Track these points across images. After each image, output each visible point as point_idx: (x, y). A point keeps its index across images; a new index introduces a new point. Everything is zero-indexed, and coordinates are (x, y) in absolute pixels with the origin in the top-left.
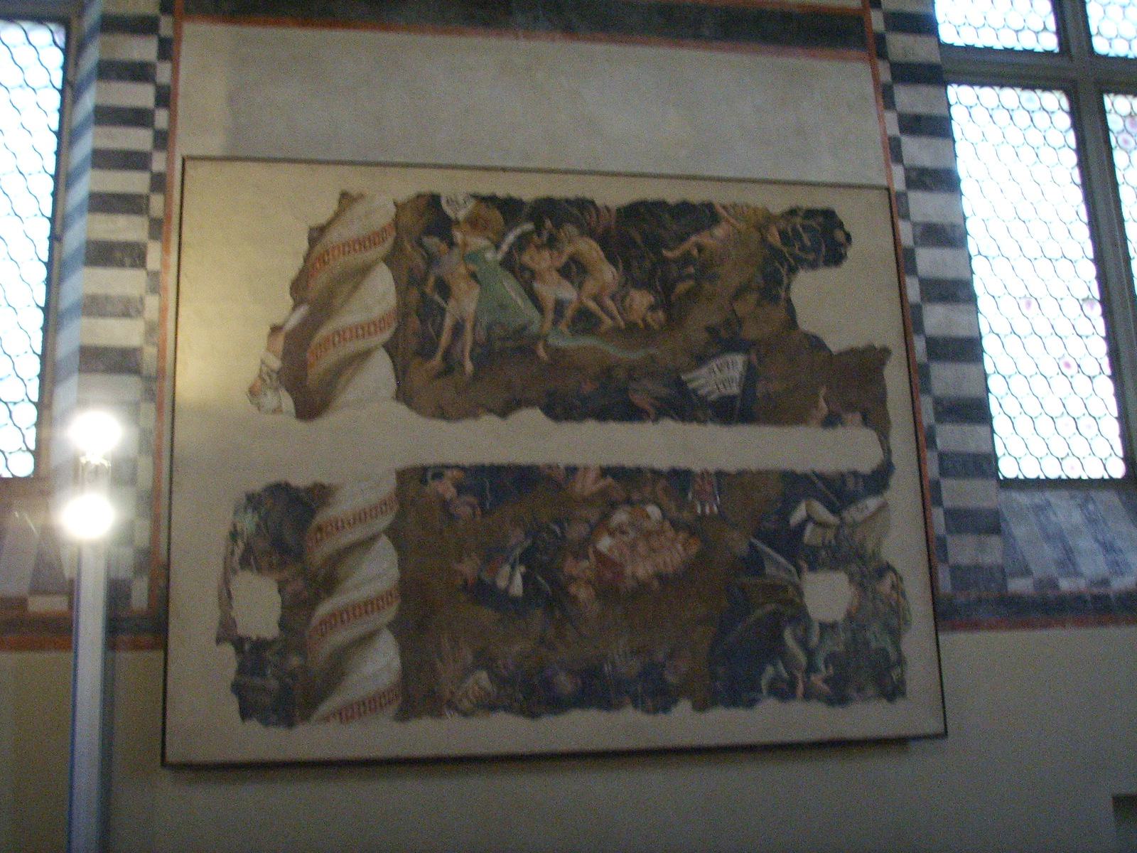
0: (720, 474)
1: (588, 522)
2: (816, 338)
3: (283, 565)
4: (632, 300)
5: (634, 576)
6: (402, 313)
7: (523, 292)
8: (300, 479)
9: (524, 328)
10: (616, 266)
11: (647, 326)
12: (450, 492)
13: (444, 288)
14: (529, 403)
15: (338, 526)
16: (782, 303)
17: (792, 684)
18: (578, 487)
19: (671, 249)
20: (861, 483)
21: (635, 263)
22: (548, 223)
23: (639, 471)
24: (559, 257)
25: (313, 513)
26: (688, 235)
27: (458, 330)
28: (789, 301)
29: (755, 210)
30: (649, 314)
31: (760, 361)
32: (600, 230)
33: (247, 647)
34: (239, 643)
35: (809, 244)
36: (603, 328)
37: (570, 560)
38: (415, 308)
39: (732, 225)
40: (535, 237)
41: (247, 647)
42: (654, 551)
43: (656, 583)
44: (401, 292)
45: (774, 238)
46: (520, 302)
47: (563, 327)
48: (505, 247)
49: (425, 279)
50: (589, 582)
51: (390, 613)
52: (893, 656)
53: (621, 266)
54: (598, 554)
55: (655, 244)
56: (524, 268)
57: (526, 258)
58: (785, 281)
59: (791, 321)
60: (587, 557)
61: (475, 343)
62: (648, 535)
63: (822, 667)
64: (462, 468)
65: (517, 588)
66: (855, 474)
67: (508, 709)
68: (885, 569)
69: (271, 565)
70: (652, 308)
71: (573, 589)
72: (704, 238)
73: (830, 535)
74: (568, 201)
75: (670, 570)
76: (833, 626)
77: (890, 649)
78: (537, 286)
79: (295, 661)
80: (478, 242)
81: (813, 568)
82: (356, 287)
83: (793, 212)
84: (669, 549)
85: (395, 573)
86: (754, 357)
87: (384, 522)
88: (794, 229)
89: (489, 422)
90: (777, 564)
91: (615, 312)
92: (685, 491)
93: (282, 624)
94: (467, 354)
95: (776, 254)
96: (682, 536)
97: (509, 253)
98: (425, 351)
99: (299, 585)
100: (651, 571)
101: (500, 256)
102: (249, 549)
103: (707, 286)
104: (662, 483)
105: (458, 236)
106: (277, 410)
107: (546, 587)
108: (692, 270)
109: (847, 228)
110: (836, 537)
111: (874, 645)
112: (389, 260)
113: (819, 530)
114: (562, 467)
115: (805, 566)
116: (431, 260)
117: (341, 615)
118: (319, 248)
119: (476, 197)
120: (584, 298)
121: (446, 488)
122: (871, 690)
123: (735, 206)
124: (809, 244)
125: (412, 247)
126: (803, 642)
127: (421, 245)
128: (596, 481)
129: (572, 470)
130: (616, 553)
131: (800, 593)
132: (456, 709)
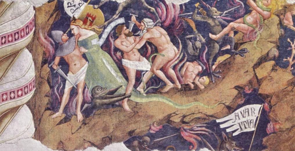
4: (187, 68)
6: (39, 81)
10: (178, 48)
11: (196, 87)
13: (65, 65)
22: (134, 18)
26: (229, 22)
27: (74, 92)
36: (166, 89)
38: (46, 78)
40: (125, 28)
44: (38, 69)
46: (113, 73)
47: (140, 89)
48: (105, 36)
53: (181, 46)
56: (116, 50)
70: (201, 74)
80: (87, 33)
98: (53, 107)
101: (102, 42)
105: (75, 30)
112: (30, 47)
116: (58, 46)
125: (46, 38)
127: (50, 35)
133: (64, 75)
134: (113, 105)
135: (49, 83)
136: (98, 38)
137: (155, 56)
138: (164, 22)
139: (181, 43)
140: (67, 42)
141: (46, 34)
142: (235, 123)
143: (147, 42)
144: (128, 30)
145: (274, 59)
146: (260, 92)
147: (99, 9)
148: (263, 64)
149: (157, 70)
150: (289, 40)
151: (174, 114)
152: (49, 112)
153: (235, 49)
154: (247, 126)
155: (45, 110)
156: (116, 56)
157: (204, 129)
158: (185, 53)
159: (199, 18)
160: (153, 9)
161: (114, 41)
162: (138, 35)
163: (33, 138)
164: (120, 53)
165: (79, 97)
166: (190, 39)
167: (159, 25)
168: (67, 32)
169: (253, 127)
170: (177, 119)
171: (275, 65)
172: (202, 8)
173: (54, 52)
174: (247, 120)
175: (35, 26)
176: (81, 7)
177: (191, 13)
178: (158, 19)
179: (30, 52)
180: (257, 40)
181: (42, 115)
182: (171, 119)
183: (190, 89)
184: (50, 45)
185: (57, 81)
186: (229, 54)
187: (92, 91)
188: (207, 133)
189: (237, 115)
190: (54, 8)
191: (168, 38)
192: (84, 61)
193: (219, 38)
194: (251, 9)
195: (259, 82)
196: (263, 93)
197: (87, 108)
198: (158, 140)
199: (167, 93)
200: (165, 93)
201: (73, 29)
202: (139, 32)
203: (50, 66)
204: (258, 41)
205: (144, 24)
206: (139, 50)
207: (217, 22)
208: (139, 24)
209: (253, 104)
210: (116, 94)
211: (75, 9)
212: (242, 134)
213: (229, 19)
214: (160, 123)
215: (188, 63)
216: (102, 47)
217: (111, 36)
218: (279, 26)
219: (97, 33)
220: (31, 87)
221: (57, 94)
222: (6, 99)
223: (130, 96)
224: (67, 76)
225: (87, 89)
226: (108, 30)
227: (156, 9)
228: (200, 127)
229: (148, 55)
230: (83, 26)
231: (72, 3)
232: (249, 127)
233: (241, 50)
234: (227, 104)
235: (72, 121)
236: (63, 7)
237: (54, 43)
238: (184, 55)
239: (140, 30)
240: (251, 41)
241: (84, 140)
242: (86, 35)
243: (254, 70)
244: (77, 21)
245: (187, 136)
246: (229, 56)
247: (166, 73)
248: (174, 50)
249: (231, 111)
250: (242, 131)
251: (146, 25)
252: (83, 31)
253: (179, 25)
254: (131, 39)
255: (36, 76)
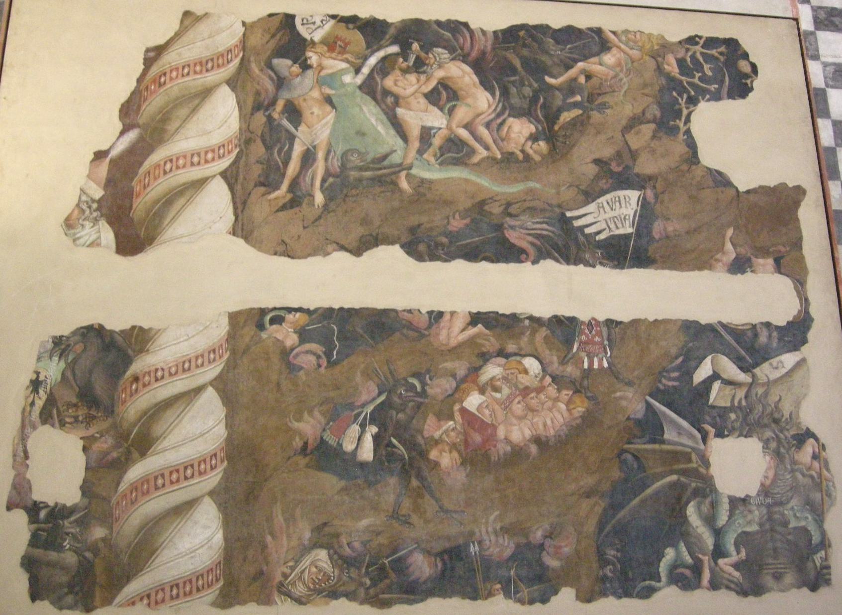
0: (609, 323)
1: (454, 376)
2: (720, 173)
3: (90, 420)
4: (510, 127)
5: (507, 440)
6: (245, 139)
7: (384, 117)
8: (116, 323)
9: (385, 157)
10: (493, 94)
11: (527, 157)
12: (292, 339)
13: (294, 113)
14: (390, 242)
15: (158, 375)
16: (681, 137)
17: (697, 569)
18: (443, 336)
19: (555, 77)
20: (775, 334)
21: (513, 90)
22: (415, 46)
23: (514, 317)
24: (428, 79)
25: (127, 361)
26: (576, 61)
27: (308, 158)
28: (688, 132)
29: (650, 35)
30: (529, 143)
31: (656, 196)
32: (474, 54)
33: (43, 514)
34: (33, 509)
35: (710, 73)
36: (476, 159)
37: (431, 420)
38: (259, 134)
39: (625, 53)
40: (401, 60)
41: (43, 514)
42: (532, 410)
43: (534, 449)
44: (245, 117)
45: (672, 66)
46: (380, 128)
47: (428, 156)
48: (366, 70)
49: (273, 103)
50: (454, 446)
51: (213, 479)
52: (816, 539)
53: (498, 93)
54: (464, 411)
55: (537, 69)
56: (386, 93)
57: (389, 82)
58: (685, 112)
59: (693, 156)
60: (451, 417)
61: (328, 174)
62: (526, 391)
63: (732, 549)
64: (308, 312)
65: (367, 452)
66: (768, 325)
67: (350, 596)
68: (805, 436)
69: (76, 418)
70: (534, 138)
71: (433, 455)
72: (591, 65)
73: (741, 393)
74: (438, 23)
75: (552, 432)
76: (745, 501)
77: (812, 528)
78: (400, 111)
79: (98, 533)
80: (334, 64)
81: (720, 435)
82: (194, 110)
83: (692, 40)
84: (550, 410)
85: (221, 431)
86: (649, 193)
87: (213, 371)
88: (693, 57)
89: (341, 258)
90: (680, 430)
91: (490, 141)
92: (569, 343)
93: (86, 489)
94: (318, 183)
95: (673, 84)
96: (566, 394)
97: (371, 76)
98: (269, 183)
99: (105, 444)
100: (528, 433)
101: (359, 79)
102: (51, 401)
103: (596, 116)
104: (543, 332)
105: (313, 58)
106: (95, 244)
107: (402, 449)
108: (578, 98)
109: (752, 59)
110: (746, 397)
111: (793, 524)
112: (232, 83)
113: (728, 390)
114: (424, 311)
115: (712, 431)
116: (281, 82)
117: (156, 478)
118: (155, 70)
119: (333, 17)
120: (454, 126)
121: (286, 334)
122: (789, 579)
123: (626, 32)
124: (710, 73)
125: (261, 70)
126: (710, 520)
127: (270, 66)
128: (463, 330)
129: (436, 316)
130: (487, 412)
131: (707, 465)
132: (289, 595)
133: (293, 130)
134: (380, 181)
135: (264, 141)
136: (354, 72)
137: (455, 106)
138: (469, 54)
139: (499, 87)
140: (299, 78)
141: (262, 64)
142: (599, 219)
143: (439, 83)
144: (406, 63)
145: (654, 121)
146: (637, 170)
147: (356, 30)
148: (637, 128)
149: (458, 127)
150: (675, 94)
151: (491, 201)
152: (262, 189)
153: (588, 101)
154: (620, 225)
155: (256, 186)
156: (384, 102)
157: (545, 226)
158: (506, 104)
159: (525, 52)
160: (449, 35)
161: (382, 79)
162: (424, 72)
163: (230, 233)
164: (392, 98)
165: (317, 167)
166: (513, 82)
167: (459, 60)
168: (299, 62)
169: (630, 227)
170: (496, 209)
171: (655, 132)
172: (529, 37)
173: (275, 90)
174: (619, 216)
175: (244, 51)
176: (326, 26)
177: (513, 44)
178: (457, 50)
179: (233, 90)
180: (623, 91)
181: (250, 194)
182: (486, 208)
183: (517, 161)
184: (267, 79)
185: (279, 140)
186: (579, 108)
187: (342, 158)
188: (550, 234)
189: (601, 205)
190: (277, 24)
191: (476, 79)
192: (328, 108)
193: (561, 84)
194: (609, 45)
195: (634, 155)
196: (640, 172)
197: (331, 185)
198: (464, 242)
199: (478, 164)
200: (474, 164)
201: (310, 58)
202: (425, 68)
203: (267, 114)
204: (625, 92)
205: (435, 57)
206: (426, 96)
207: (556, 60)
208: (426, 56)
209: (626, 189)
210: (386, 163)
211: (313, 27)
212: (613, 237)
213: (576, 56)
214: (466, 213)
215: (511, 119)
216: (360, 87)
217: (377, 73)
218: (657, 73)
219: (351, 65)
220: (230, 147)
221: (279, 160)
222: (184, 166)
223: (410, 167)
224: (297, 130)
225: (332, 153)
226: (373, 61)
227: (454, 36)
228: (537, 223)
229: (441, 103)
230: (328, 55)
231: (310, 18)
232: (623, 226)
233: (600, 104)
234: (582, 187)
235: (304, 205)
236: (293, 26)
237: (275, 78)
238: (504, 105)
239: (427, 65)
240: (614, 91)
241: (327, 239)
242: (331, 67)
243: (624, 136)
244: (317, 46)
245: (517, 238)
246: (580, 112)
247: (473, 133)
248: (488, 100)
249: (590, 200)
250: (612, 233)
251: (438, 59)
252: (328, 62)
253: (493, 60)
254: (412, 78)
255: (240, 129)
